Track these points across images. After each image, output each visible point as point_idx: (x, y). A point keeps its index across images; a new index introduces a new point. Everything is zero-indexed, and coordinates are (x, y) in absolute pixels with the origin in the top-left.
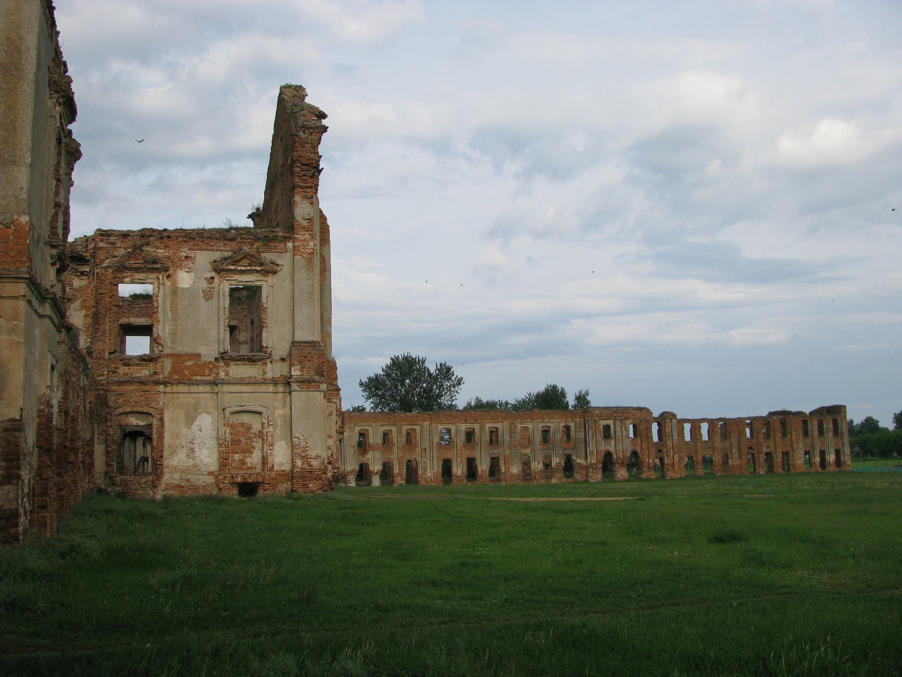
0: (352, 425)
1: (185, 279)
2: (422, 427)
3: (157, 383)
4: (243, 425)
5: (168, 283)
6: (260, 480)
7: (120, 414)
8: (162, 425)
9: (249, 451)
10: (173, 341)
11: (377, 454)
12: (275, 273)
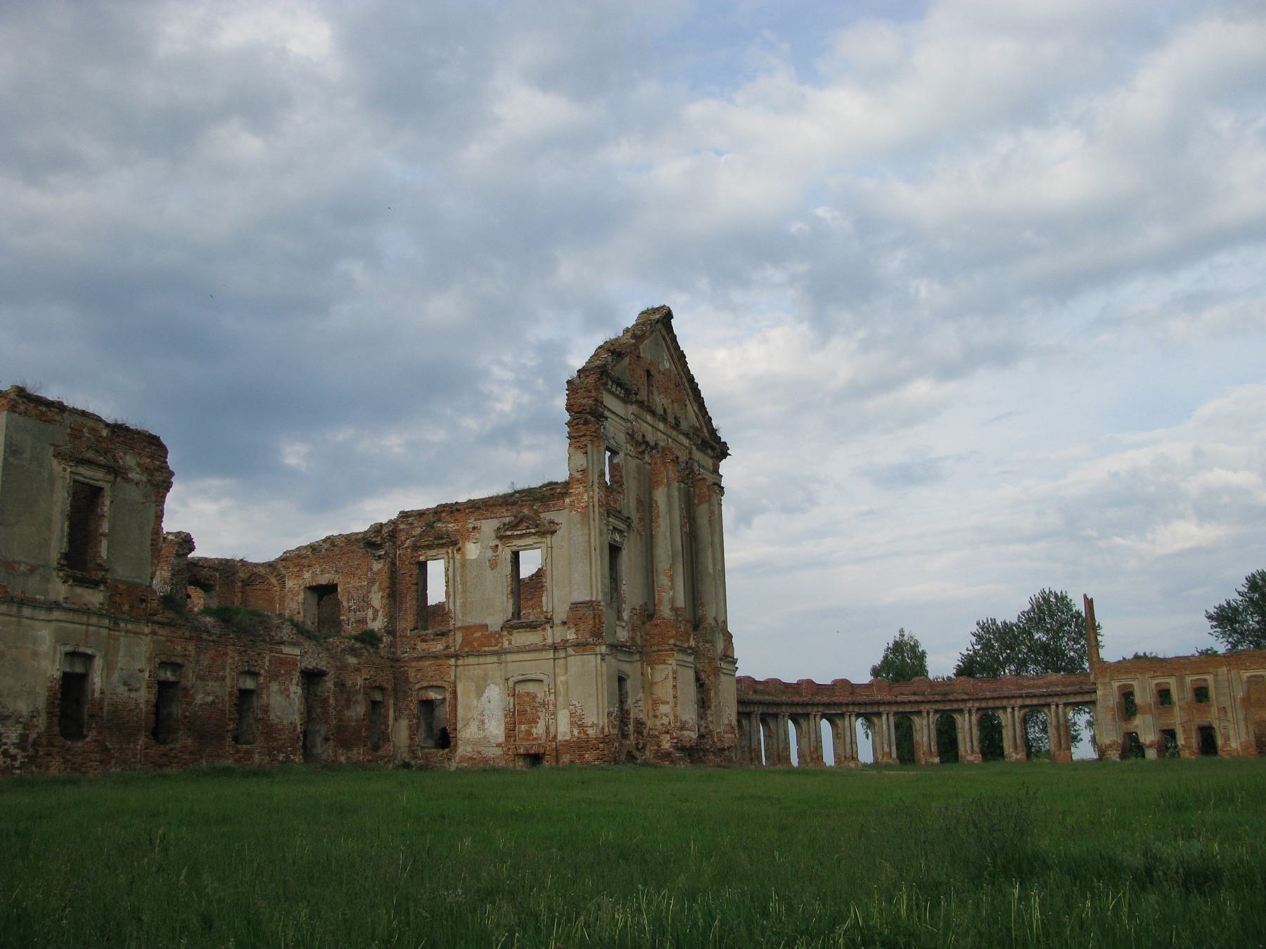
0: (1107, 680)
1: (472, 550)
2: (1216, 675)
3: (449, 657)
4: (528, 694)
5: (458, 557)
6: (542, 751)
7: (421, 689)
8: (455, 698)
9: (534, 721)
10: (464, 614)
11: (1149, 718)
12: (553, 533)
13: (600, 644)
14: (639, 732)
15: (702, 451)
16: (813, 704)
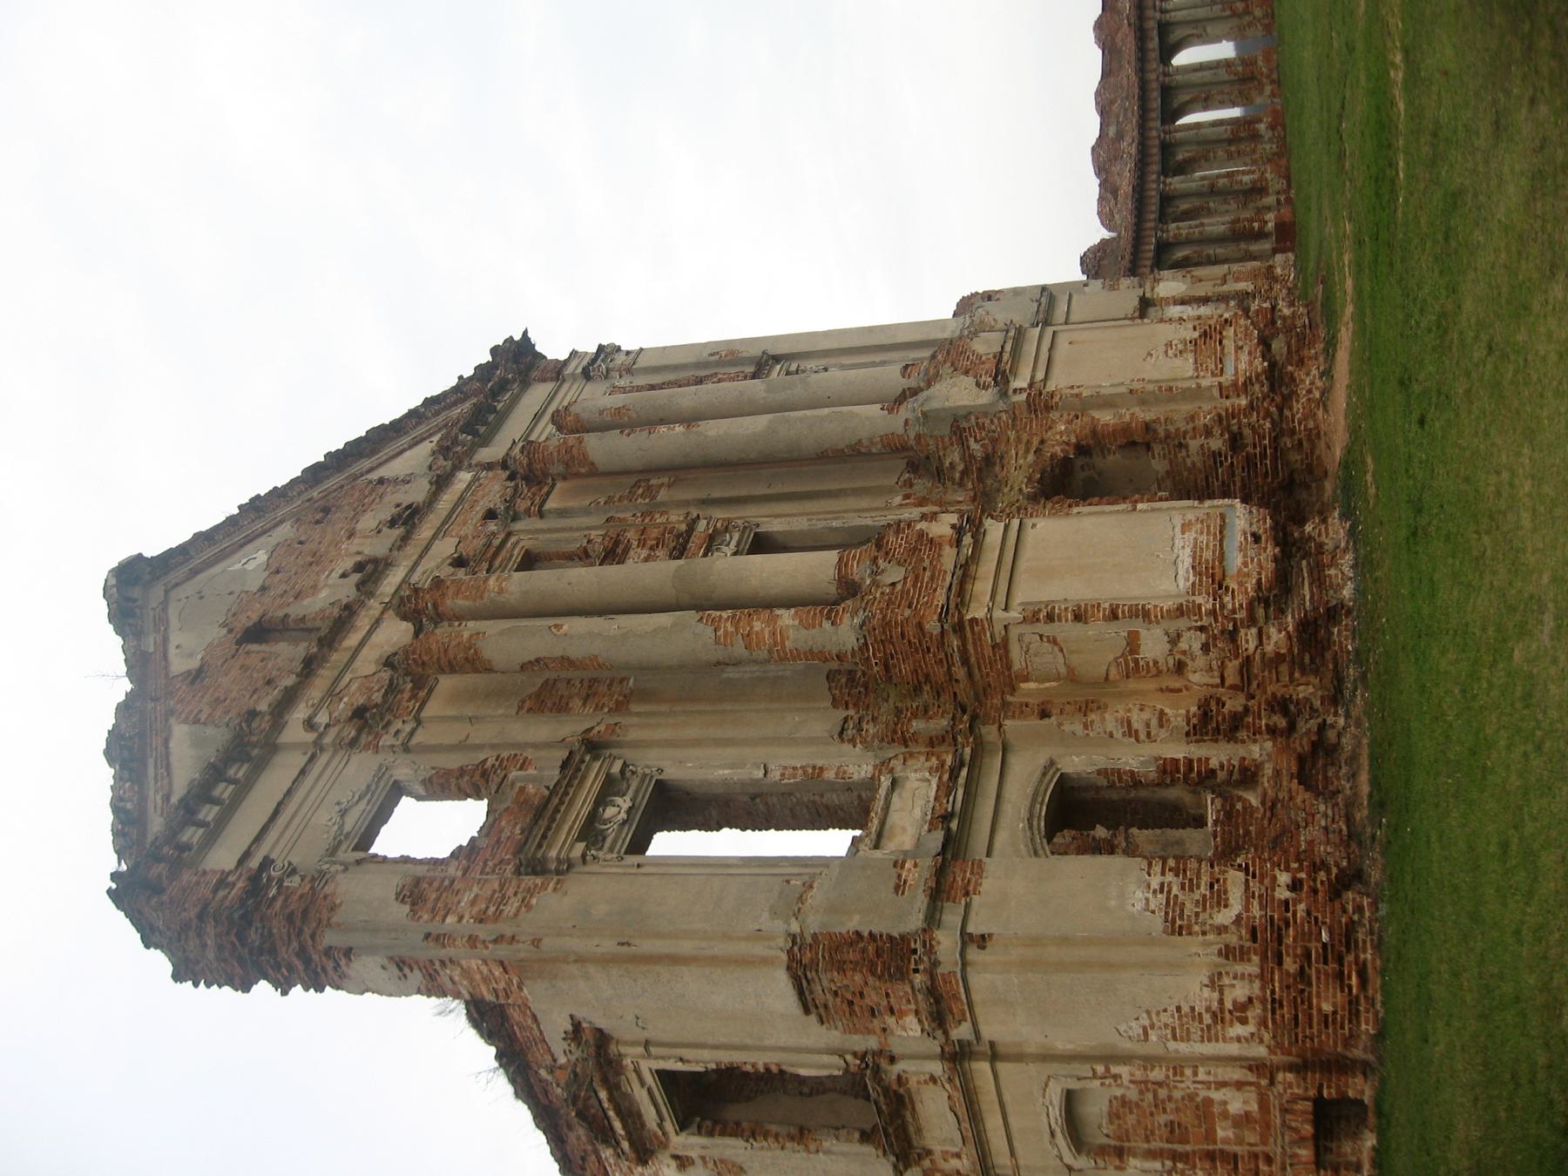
4: (1114, 1116)
13: (930, 950)
14: (1233, 728)
15: (495, 429)
16: (1141, 18)
